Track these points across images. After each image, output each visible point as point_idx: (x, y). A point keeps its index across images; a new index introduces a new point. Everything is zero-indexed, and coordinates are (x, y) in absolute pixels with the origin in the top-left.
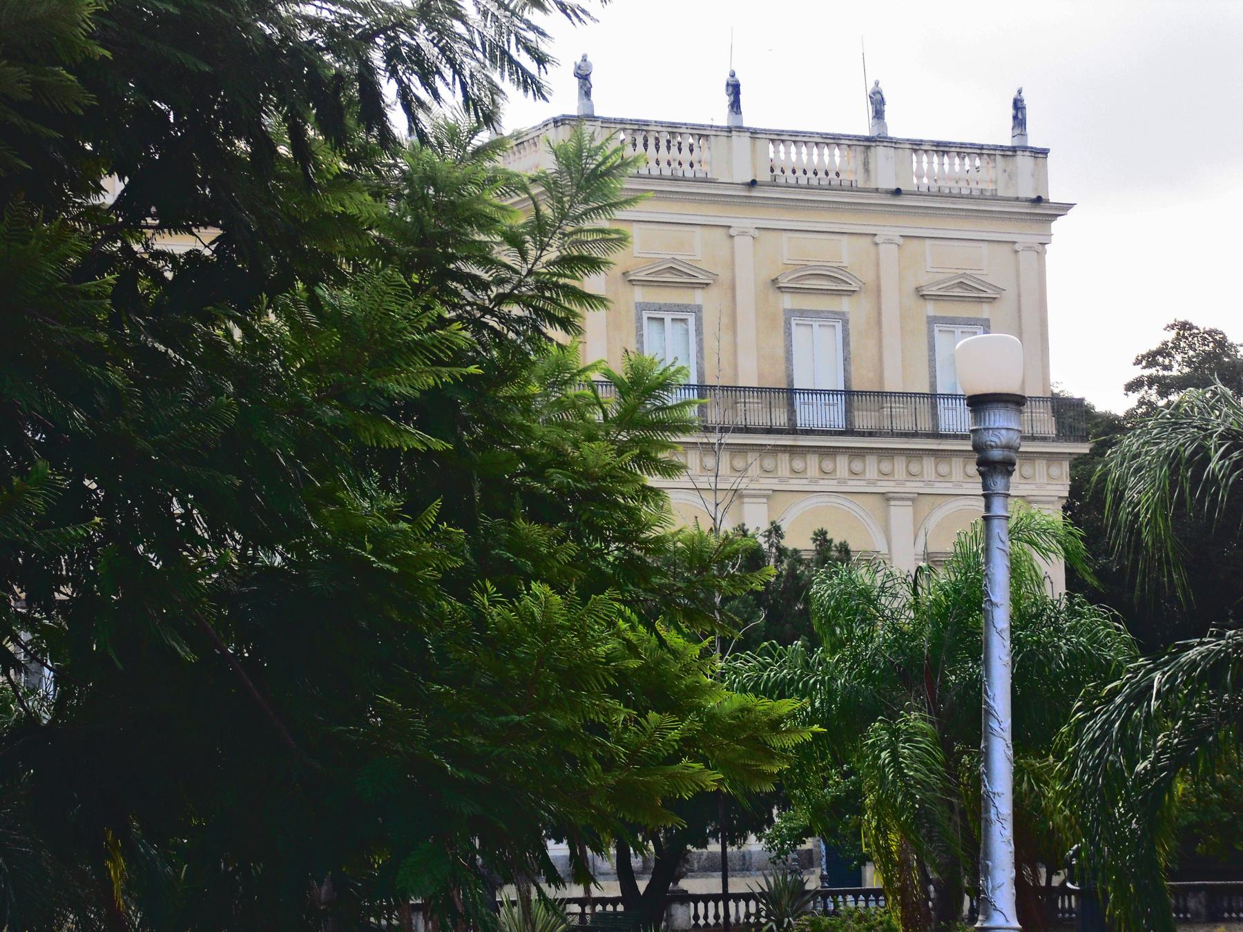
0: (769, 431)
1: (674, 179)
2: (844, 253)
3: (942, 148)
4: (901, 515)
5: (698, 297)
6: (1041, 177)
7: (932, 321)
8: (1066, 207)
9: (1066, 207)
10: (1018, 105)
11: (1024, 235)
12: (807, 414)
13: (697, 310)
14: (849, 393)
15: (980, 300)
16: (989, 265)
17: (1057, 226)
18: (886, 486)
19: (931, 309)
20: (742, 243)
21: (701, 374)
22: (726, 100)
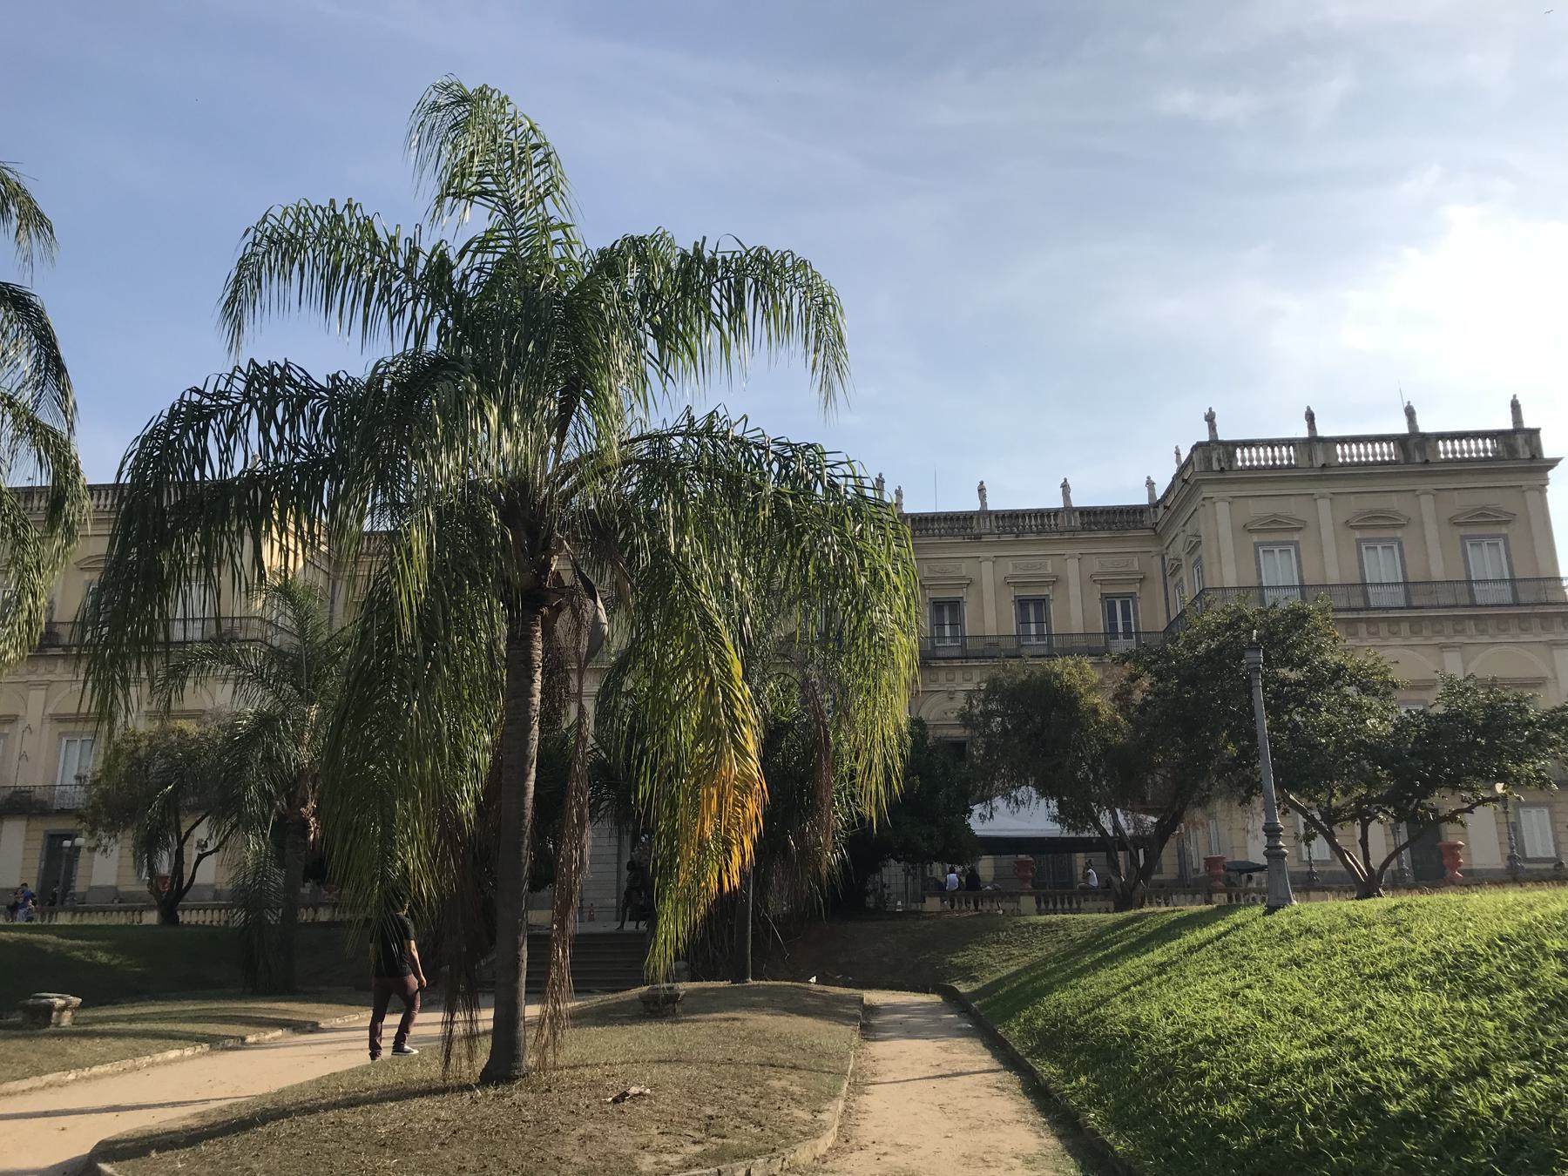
2: (1394, 503)
5: (1296, 537)
8: (1554, 462)
9: (1554, 462)
11: (1525, 481)
13: (1296, 544)
14: (1406, 583)
15: (1498, 523)
17: (1550, 473)
18: (1443, 640)
21: (1301, 578)
22: (1306, 423)
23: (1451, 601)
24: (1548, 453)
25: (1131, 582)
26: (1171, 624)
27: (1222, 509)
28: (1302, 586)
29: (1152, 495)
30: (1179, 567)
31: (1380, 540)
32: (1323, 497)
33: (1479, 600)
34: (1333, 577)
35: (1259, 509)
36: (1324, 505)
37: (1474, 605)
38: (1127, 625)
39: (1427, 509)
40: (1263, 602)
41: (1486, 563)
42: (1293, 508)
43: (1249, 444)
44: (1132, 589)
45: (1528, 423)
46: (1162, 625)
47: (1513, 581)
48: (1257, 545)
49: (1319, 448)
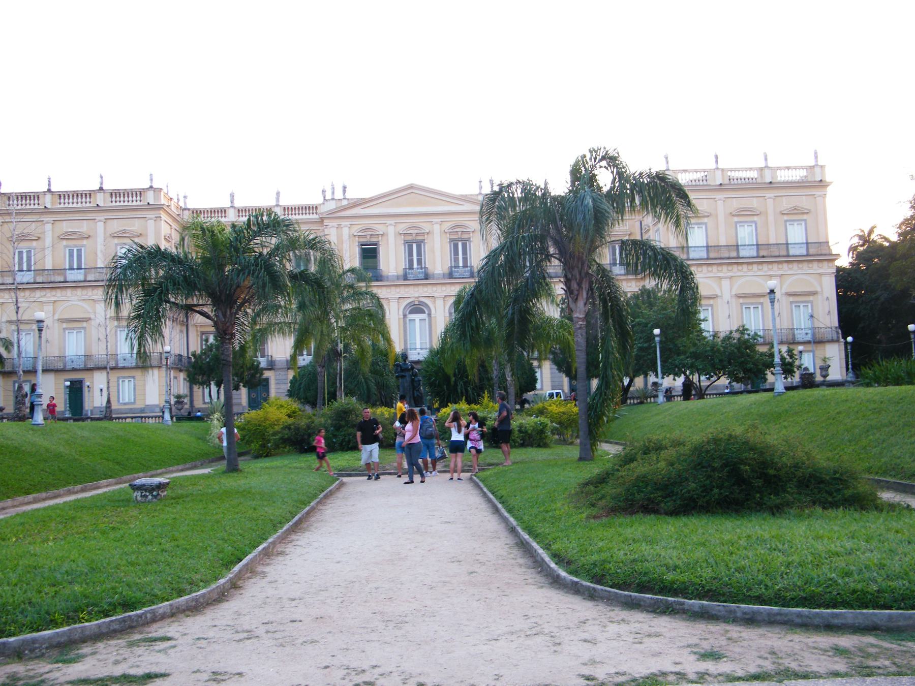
0: (729, 258)
1: (696, 186)
2: (754, 203)
3: (788, 168)
4: (726, 283)
6: (823, 173)
7: (786, 221)
10: (816, 153)
11: (817, 192)
12: (743, 253)
13: (706, 224)
14: (757, 245)
16: (804, 203)
17: (829, 188)
19: (786, 218)
20: (720, 203)
21: (707, 243)
23: (777, 254)
24: (828, 179)
28: (707, 247)
30: (649, 230)
31: (746, 222)
32: (720, 200)
33: (791, 253)
34: (723, 242)
36: (720, 204)
37: (788, 256)
39: (770, 203)
40: (688, 253)
41: (796, 234)
43: (685, 171)
45: (820, 163)
47: (807, 243)
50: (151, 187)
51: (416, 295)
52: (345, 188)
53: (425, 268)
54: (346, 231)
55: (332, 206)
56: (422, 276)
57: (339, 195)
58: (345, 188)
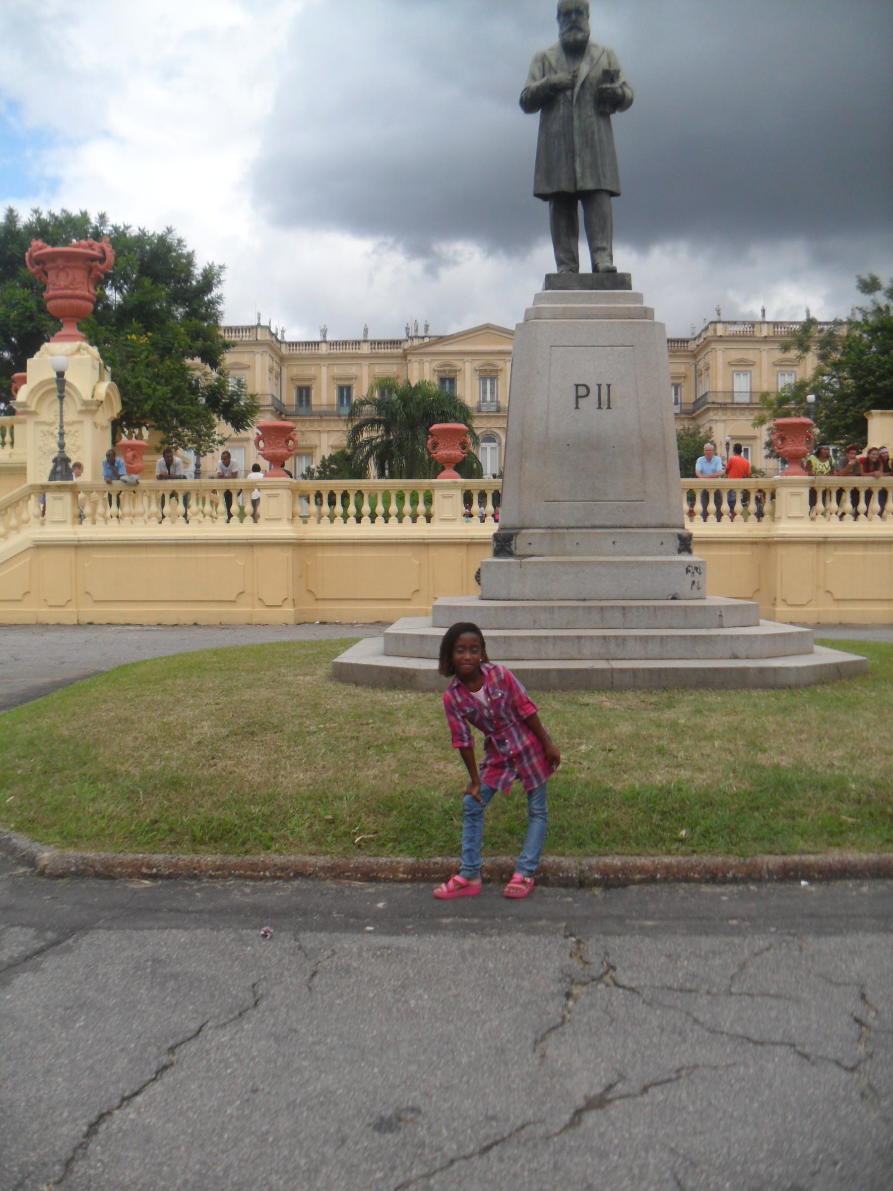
5: (751, 368)
13: (750, 372)
25: (681, 377)
26: (697, 401)
27: (720, 354)
28: (751, 392)
29: (693, 334)
35: (735, 355)
36: (764, 354)
38: (676, 399)
40: (733, 397)
42: (750, 355)
43: (735, 323)
44: (679, 381)
46: (693, 400)
48: (734, 371)
49: (765, 326)
50: (259, 325)
51: (489, 426)
52: (427, 327)
53: (497, 401)
54: (427, 366)
55: (416, 342)
56: (494, 409)
57: (421, 333)
58: (427, 327)
